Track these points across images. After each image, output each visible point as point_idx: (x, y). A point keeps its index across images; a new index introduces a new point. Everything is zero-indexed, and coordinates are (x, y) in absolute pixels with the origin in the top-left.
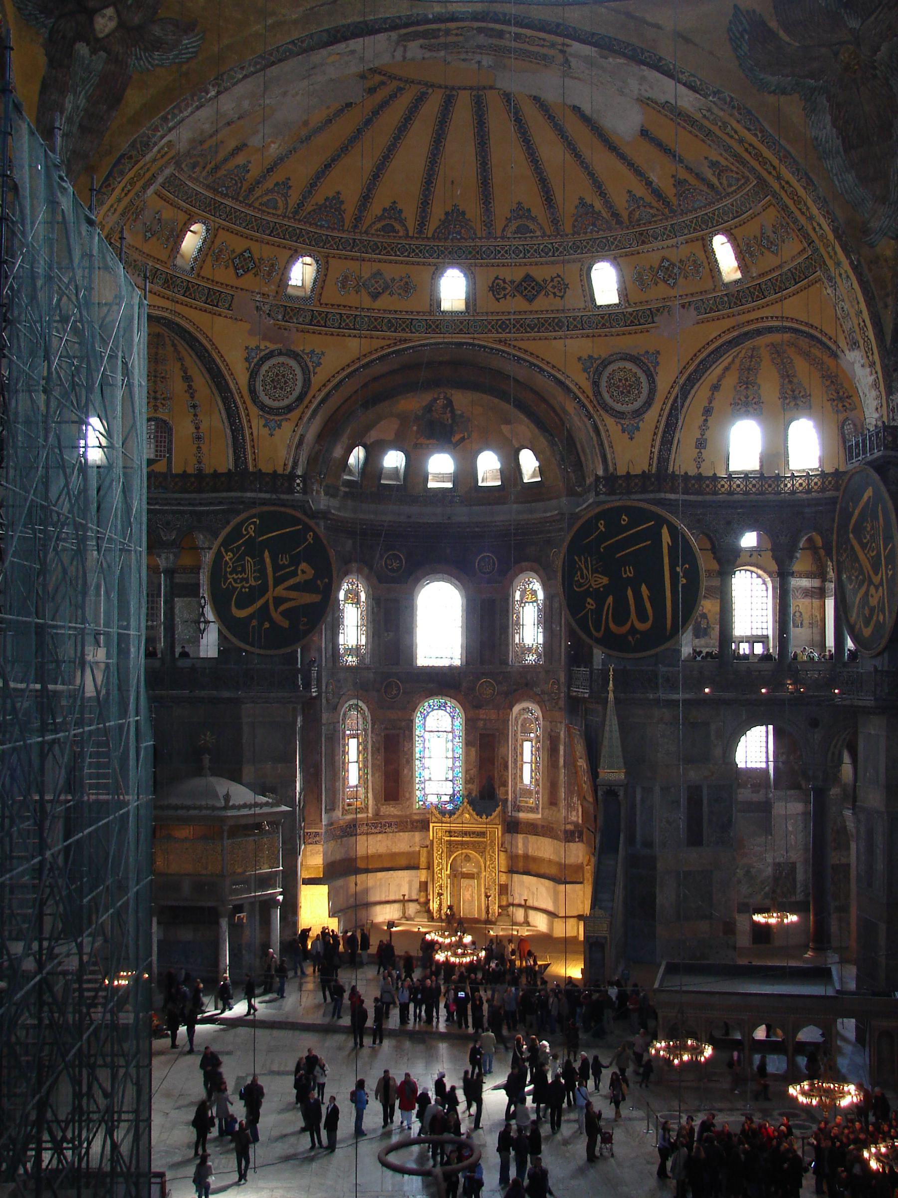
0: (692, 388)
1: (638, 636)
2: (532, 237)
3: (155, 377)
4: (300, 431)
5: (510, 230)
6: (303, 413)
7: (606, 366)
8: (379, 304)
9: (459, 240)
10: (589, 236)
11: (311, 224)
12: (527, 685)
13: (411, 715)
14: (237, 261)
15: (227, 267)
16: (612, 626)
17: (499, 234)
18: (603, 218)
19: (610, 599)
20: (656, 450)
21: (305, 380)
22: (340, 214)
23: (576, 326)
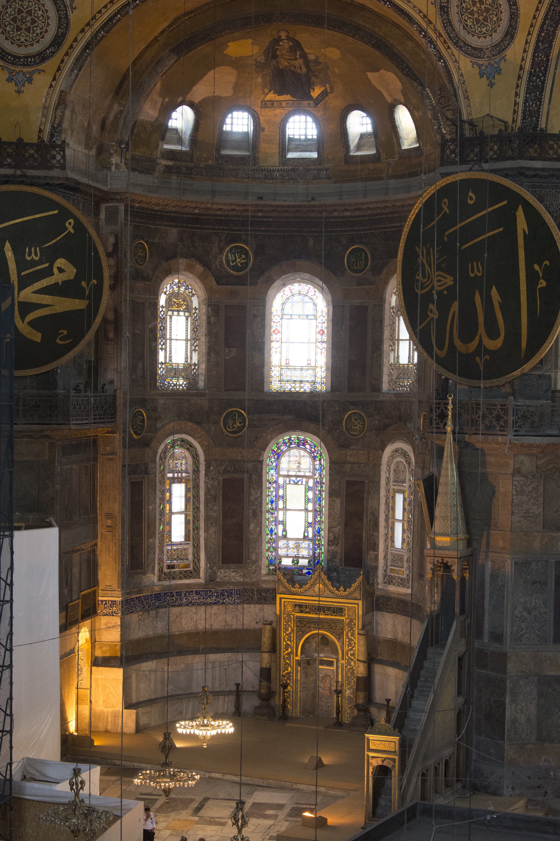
4: (60, 85)
6: (62, 61)
13: (260, 455)
16: (457, 343)
19: (455, 307)
20: (521, 100)
21: (60, 18)
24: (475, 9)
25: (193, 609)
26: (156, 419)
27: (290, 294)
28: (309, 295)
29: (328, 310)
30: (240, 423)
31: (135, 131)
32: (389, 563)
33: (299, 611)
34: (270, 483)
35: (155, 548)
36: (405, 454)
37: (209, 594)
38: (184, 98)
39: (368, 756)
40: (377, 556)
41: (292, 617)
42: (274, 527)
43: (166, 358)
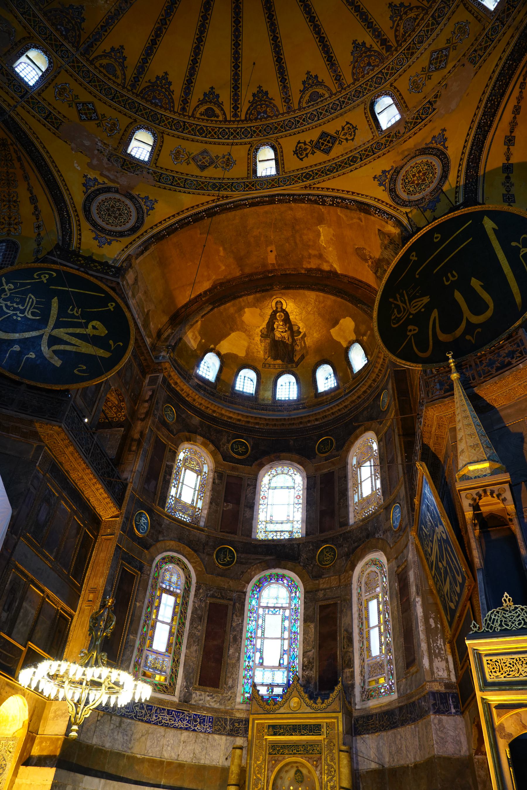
0: (485, 138)
1: (479, 330)
2: (322, 101)
3: (9, 201)
5: (305, 101)
6: (134, 240)
7: (399, 172)
8: (206, 173)
9: (266, 118)
10: (367, 77)
11: (147, 101)
12: (368, 536)
13: (244, 586)
14: (80, 107)
15: (70, 106)
16: (442, 337)
17: (296, 107)
18: (375, 51)
19: (435, 313)
21: (138, 218)
22: (170, 95)
23: (368, 155)
24: (415, 178)
25: (162, 730)
26: (160, 532)
27: (275, 473)
28: (290, 473)
29: (304, 483)
30: (230, 558)
31: (180, 345)
32: (366, 676)
33: (272, 733)
34: (251, 613)
35: (134, 646)
36: (374, 562)
37: (181, 717)
38: (215, 346)
39: (487, 704)
40: (353, 672)
41: (264, 743)
42: (251, 654)
43: (176, 494)
